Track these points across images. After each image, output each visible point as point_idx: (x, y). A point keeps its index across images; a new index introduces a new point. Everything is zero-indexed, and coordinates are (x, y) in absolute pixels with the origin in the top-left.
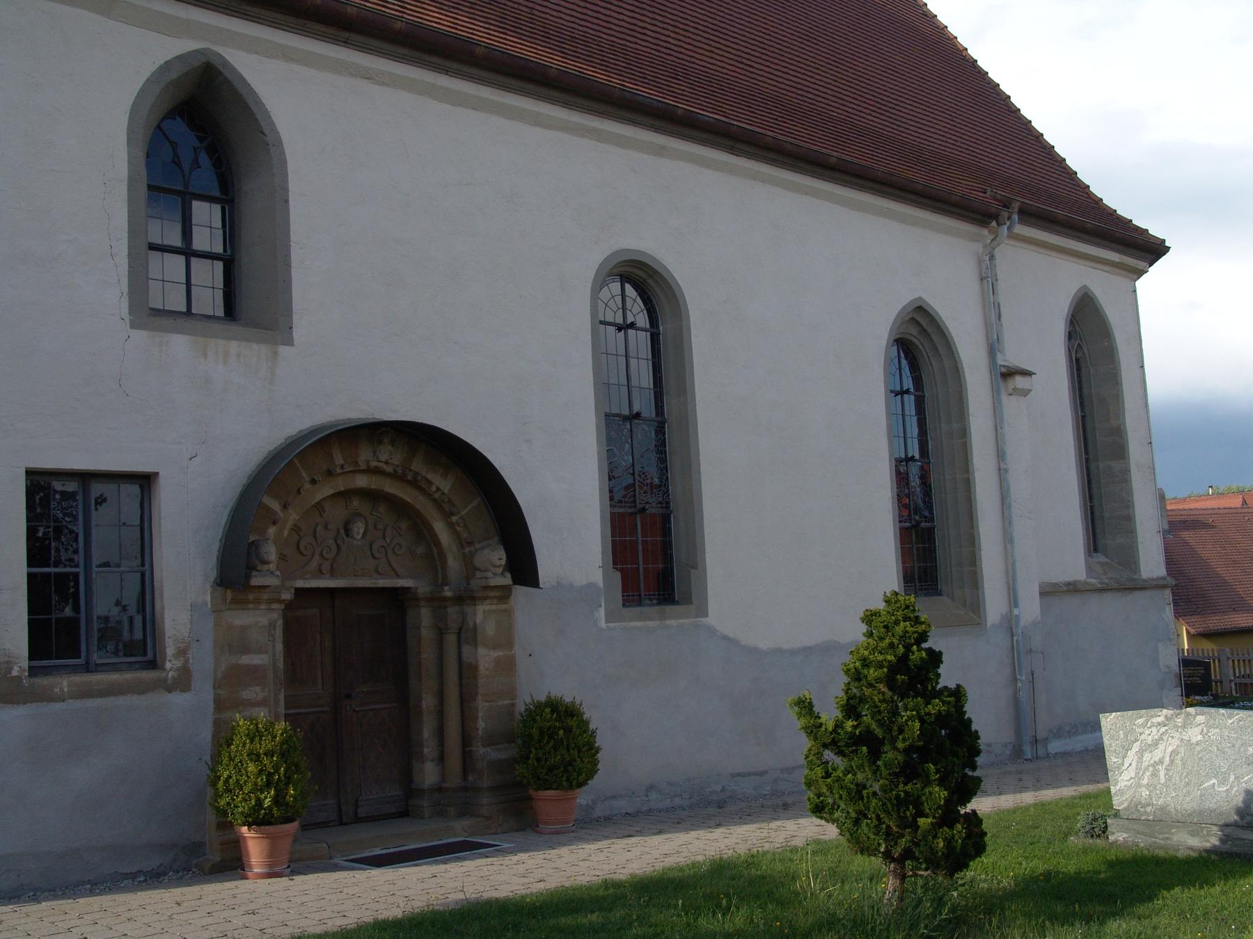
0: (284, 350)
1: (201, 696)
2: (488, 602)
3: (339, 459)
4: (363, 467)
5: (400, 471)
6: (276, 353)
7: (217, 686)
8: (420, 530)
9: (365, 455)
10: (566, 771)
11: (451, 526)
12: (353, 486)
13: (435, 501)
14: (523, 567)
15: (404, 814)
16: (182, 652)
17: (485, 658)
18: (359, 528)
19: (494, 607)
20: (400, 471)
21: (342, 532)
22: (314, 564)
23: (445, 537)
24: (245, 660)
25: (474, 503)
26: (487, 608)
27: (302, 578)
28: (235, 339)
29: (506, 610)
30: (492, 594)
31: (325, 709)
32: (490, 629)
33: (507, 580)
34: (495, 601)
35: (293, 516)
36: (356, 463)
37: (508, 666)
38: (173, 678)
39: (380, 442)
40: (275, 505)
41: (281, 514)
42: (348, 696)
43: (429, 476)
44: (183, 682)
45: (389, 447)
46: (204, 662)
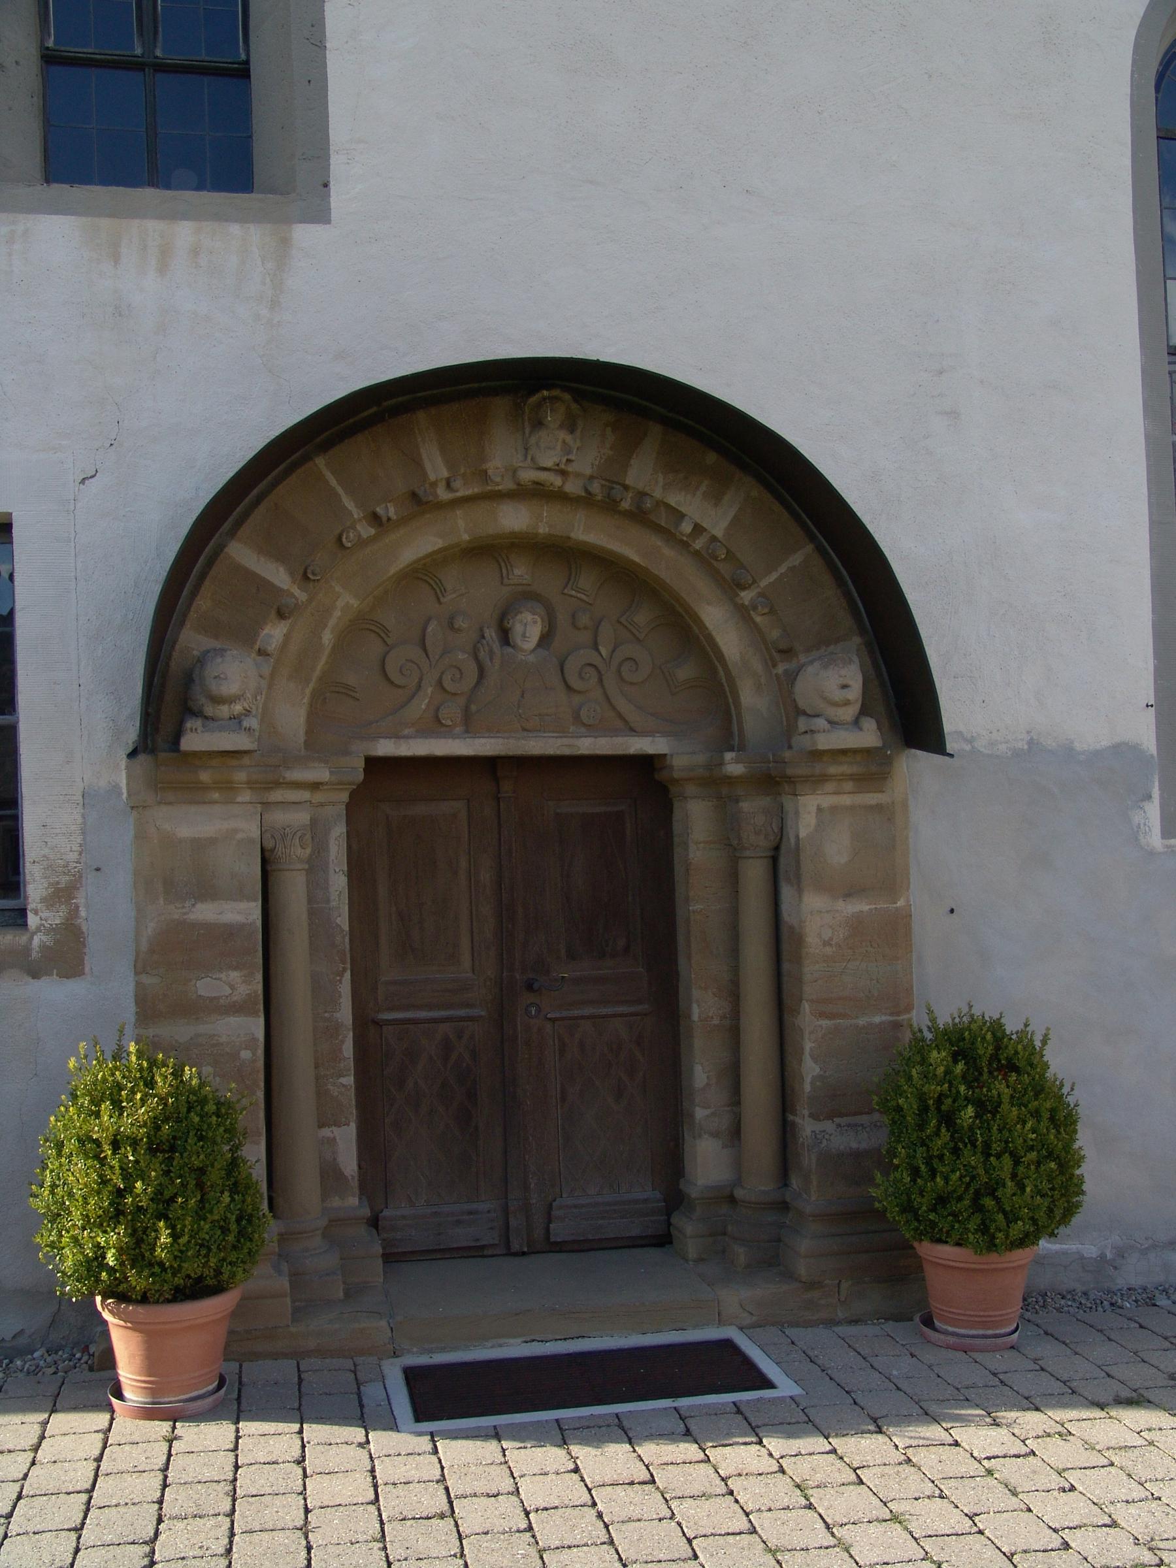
0: (305, 234)
1: (107, 988)
2: (830, 786)
3: (436, 467)
4: (508, 485)
5: (596, 488)
6: (285, 242)
7: (141, 967)
9: (504, 455)
10: (977, 1207)
11: (743, 613)
14: (909, 707)
15: (663, 1240)
16: (62, 894)
17: (818, 916)
18: (528, 628)
19: (846, 800)
20: (596, 488)
21: (491, 634)
22: (421, 705)
23: (731, 641)
24: (205, 912)
25: (796, 559)
26: (827, 801)
27: (397, 736)
28: (185, 217)
29: (879, 808)
30: (833, 770)
31: (475, 1012)
32: (837, 850)
33: (869, 736)
34: (849, 786)
35: (345, 601)
36: (484, 476)
37: (894, 933)
38: (44, 947)
39: (538, 424)
40: (279, 576)
41: (302, 596)
42: (530, 987)
43: (674, 499)
44: (66, 956)
45: (563, 435)
46: (114, 915)
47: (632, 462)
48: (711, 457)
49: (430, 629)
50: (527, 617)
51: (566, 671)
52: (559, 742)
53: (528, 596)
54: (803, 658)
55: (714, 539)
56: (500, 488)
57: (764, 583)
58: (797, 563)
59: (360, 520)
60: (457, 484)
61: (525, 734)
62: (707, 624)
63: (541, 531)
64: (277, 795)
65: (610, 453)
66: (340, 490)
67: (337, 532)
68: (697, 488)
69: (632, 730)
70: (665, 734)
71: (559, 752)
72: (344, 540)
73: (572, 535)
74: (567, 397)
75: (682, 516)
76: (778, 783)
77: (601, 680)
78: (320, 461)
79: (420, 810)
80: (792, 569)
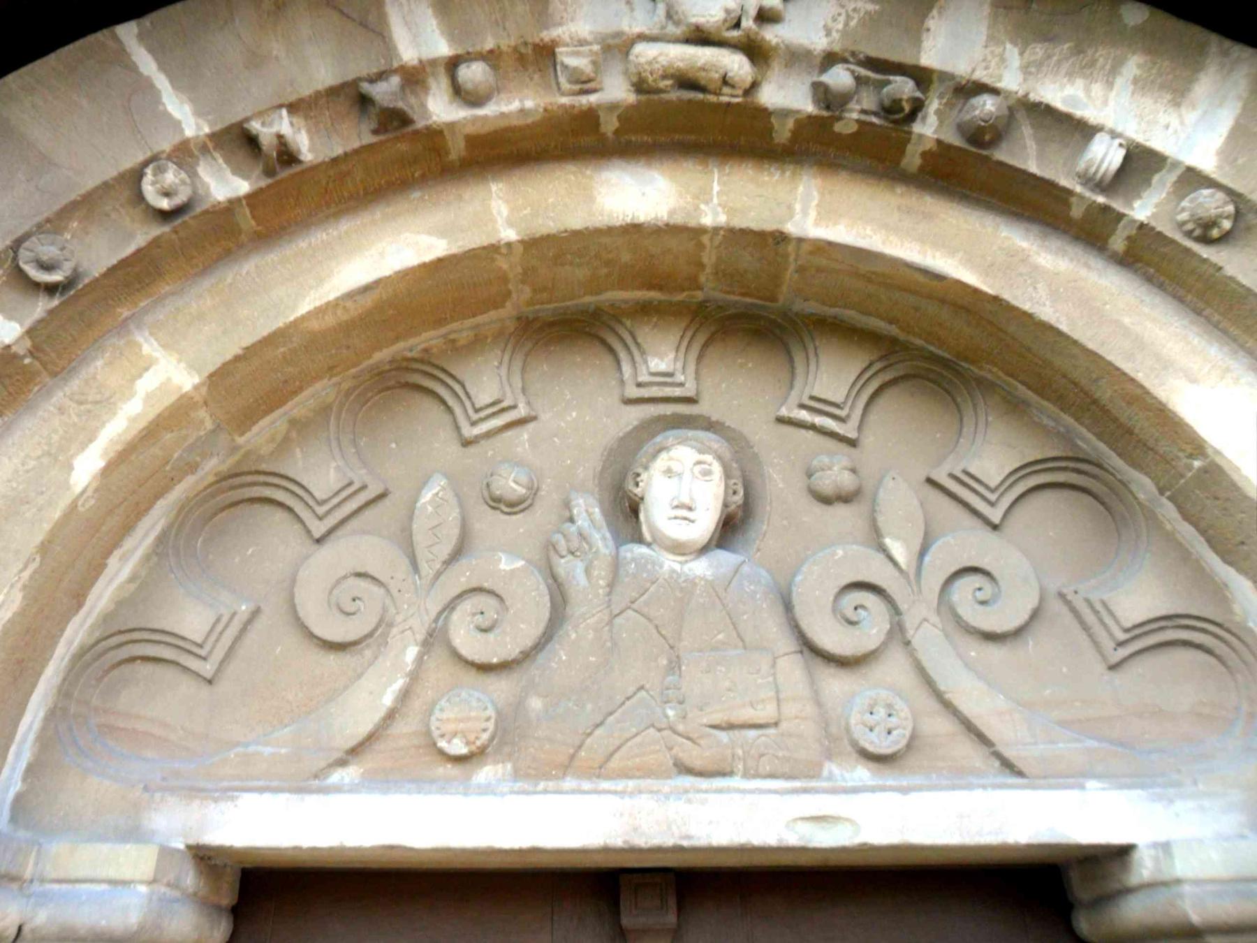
4: (615, 90)
12: (576, 220)
18: (684, 487)
21: (589, 512)
43: (1058, 93)
47: (931, 23)
49: (427, 496)
51: (798, 610)
53: (678, 416)
55: (1192, 179)
56: (593, 98)
59: (204, 149)
60: (474, 73)
61: (688, 781)
63: (707, 220)
67: (129, 162)
68: (1114, 71)
69: (1008, 766)
72: (149, 189)
73: (791, 228)
75: (1083, 131)
77: (898, 633)
78: (127, 32)
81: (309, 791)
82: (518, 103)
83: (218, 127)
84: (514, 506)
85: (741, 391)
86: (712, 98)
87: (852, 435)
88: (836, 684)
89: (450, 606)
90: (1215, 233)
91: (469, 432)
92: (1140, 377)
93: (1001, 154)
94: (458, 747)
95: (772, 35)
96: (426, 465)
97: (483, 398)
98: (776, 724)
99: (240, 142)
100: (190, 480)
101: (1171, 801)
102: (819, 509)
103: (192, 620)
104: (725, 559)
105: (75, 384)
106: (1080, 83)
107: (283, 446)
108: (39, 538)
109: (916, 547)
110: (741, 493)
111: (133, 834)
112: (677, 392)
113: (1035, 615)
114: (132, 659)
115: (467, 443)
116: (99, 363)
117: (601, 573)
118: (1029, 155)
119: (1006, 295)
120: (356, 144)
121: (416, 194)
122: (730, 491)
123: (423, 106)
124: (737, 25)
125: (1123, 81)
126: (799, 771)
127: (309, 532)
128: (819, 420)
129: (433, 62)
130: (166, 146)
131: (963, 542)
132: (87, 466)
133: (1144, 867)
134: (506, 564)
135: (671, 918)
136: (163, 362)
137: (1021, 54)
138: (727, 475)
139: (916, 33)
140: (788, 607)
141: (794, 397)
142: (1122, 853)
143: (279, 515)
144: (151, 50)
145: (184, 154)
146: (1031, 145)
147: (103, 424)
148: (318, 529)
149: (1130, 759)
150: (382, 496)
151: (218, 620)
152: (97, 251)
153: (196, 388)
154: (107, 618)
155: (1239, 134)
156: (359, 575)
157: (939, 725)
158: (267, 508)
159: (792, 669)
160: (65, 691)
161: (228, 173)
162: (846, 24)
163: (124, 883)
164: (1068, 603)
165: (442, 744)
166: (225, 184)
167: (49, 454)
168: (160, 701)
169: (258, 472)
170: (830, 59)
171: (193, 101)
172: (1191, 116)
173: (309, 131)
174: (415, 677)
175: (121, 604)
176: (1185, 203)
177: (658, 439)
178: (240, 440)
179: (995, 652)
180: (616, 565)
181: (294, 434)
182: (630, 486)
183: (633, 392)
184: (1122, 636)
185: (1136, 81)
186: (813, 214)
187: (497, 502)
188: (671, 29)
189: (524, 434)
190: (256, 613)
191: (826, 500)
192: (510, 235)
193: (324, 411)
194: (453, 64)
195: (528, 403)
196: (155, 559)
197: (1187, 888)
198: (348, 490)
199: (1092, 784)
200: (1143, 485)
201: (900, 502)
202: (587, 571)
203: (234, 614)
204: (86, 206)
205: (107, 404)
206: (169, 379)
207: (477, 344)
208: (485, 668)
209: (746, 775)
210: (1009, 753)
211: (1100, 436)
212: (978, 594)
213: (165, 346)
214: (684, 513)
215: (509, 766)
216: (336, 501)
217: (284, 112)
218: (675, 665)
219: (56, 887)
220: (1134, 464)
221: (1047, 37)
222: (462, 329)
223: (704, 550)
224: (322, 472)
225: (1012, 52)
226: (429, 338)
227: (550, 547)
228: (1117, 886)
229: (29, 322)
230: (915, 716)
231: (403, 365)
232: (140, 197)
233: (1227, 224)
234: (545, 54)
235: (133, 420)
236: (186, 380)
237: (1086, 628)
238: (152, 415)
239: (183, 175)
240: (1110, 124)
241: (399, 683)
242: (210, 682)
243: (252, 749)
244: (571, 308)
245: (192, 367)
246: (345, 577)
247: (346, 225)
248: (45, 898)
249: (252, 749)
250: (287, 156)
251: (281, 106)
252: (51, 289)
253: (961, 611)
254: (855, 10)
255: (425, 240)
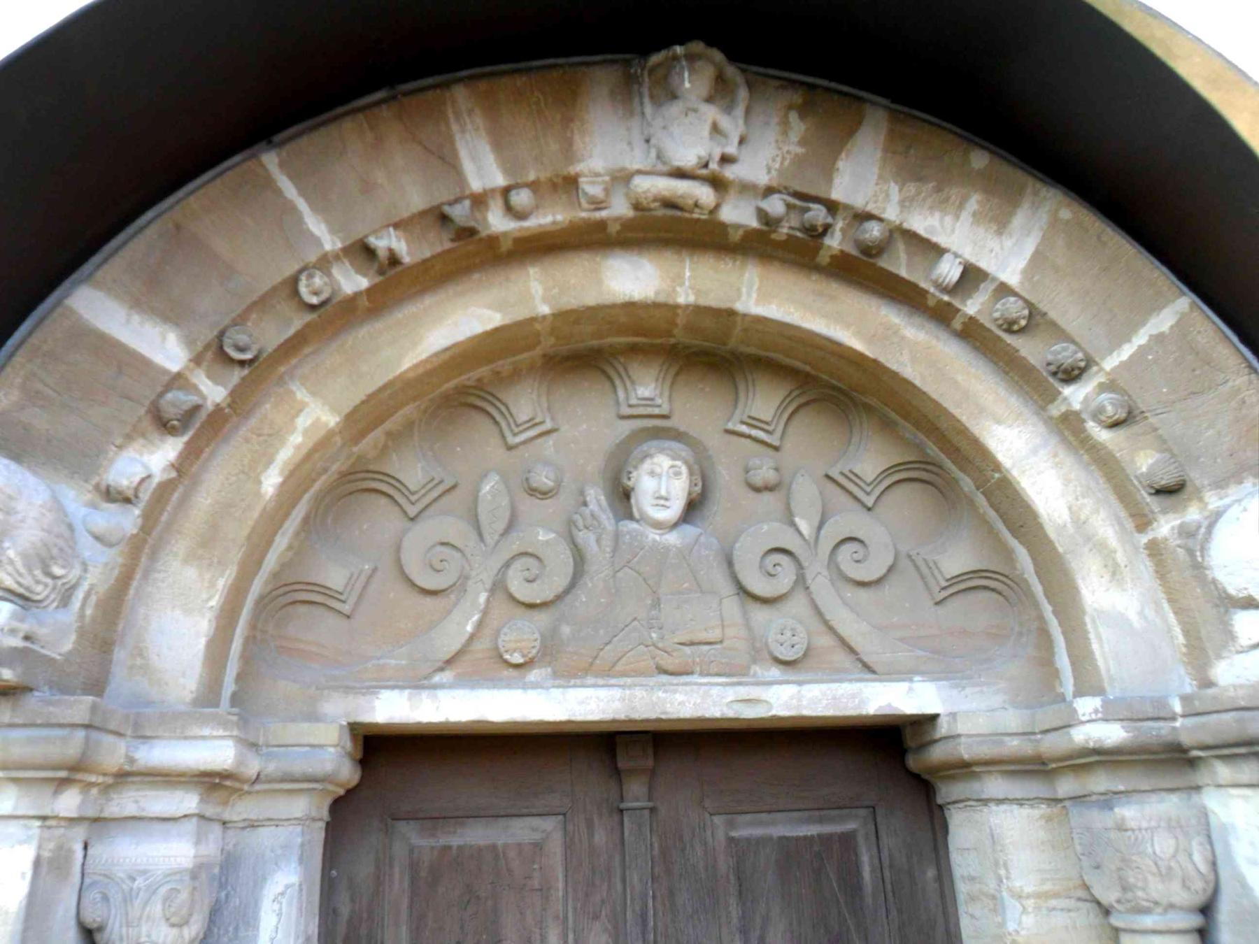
3: (482, 167)
4: (620, 208)
8: (941, 462)
11: (1069, 428)
12: (591, 299)
13: (972, 334)
18: (661, 482)
21: (597, 498)
25: (1164, 321)
40: (167, 349)
43: (921, 223)
45: (711, 113)
47: (841, 164)
48: (980, 159)
49: (486, 488)
50: (663, 462)
51: (737, 567)
52: (732, 694)
53: (659, 431)
54: (1213, 501)
55: (1003, 290)
56: (603, 214)
57: (1110, 363)
58: (1165, 328)
59: (337, 257)
60: (522, 198)
61: (665, 678)
62: (1000, 457)
63: (681, 300)
64: (127, 803)
65: (800, 150)
66: (302, 205)
68: (961, 207)
69: (868, 668)
70: (931, 675)
71: (730, 714)
72: (303, 290)
73: (739, 307)
74: (718, 56)
75: (937, 251)
76: (1192, 763)
77: (801, 581)
78: (270, 160)
79: (475, 835)
80: (1159, 339)
81: (423, 687)
82: (550, 217)
83: (348, 243)
84: (544, 494)
85: (700, 409)
86: (687, 215)
87: (776, 443)
88: (760, 615)
89: (507, 565)
90: (1016, 327)
91: (512, 440)
92: (964, 419)
93: (884, 263)
94: (517, 658)
95: (730, 172)
96: (482, 463)
97: (522, 417)
98: (721, 642)
99: (363, 252)
100: (324, 478)
101: (964, 688)
102: (752, 494)
103: (335, 577)
104: (689, 531)
105: (253, 422)
106: (937, 215)
107: (384, 451)
108: (246, 532)
109: (816, 524)
110: (700, 484)
111: (313, 717)
112: (656, 411)
113: (891, 570)
114: (295, 602)
115: (510, 448)
116: (268, 406)
117: (607, 543)
118: (900, 265)
119: (882, 360)
120: (439, 249)
121: (476, 276)
122: (693, 484)
123: (485, 219)
124: (706, 166)
125: (966, 216)
126: (734, 672)
127: (405, 513)
128: (754, 432)
129: (493, 191)
130: (312, 258)
131: (849, 521)
132: (271, 481)
133: (943, 728)
134: (542, 536)
135: (650, 762)
136: (312, 406)
137: (900, 191)
138: (691, 473)
139: (828, 172)
140: (730, 564)
141: (738, 415)
142: (933, 718)
143: (383, 501)
144: (291, 178)
145: (324, 263)
146: (903, 256)
147: (277, 451)
148: (412, 511)
149: (941, 663)
150: (454, 487)
151: (352, 575)
152: (269, 334)
153: (338, 424)
154: (275, 575)
155: (1038, 259)
156: (443, 544)
157: (825, 641)
158: (374, 496)
159: (732, 606)
160: (253, 626)
161: (352, 272)
162: (782, 163)
163: (321, 746)
164: (913, 561)
165: (507, 657)
166: (352, 282)
167: (243, 472)
168: (317, 630)
169: (368, 471)
170: (769, 191)
171: (327, 222)
172: (1008, 243)
173: (407, 242)
174: (485, 613)
175: (284, 566)
176: (998, 306)
177: (645, 447)
178: (355, 449)
179: (863, 594)
180: (617, 536)
181: (390, 443)
182: (625, 481)
183: (626, 411)
184: (944, 584)
185: (974, 215)
186: (754, 295)
187: (533, 492)
188: (660, 167)
189: (550, 441)
190: (375, 570)
191: (757, 490)
192: (545, 310)
193: (410, 425)
194: (506, 191)
195: (553, 419)
196: (303, 534)
197: (963, 740)
198: (432, 483)
199: (917, 678)
200: (967, 483)
201: (806, 491)
202: (598, 541)
203: (361, 571)
204: (262, 303)
205: (277, 436)
206: (318, 419)
207: (515, 375)
208: (531, 606)
209: (702, 674)
210: (865, 659)
211: (941, 449)
212: (855, 556)
213: (313, 394)
214: (662, 502)
215: (549, 670)
216: (423, 491)
217: (391, 229)
218: (657, 604)
219: (275, 749)
220: (962, 469)
221: (920, 179)
222: (505, 365)
223: (675, 525)
224: (413, 470)
225: (894, 189)
226: (483, 371)
227: (571, 523)
228: (929, 738)
229: (231, 386)
230: (809, 634)
231: (462, 391)
232: (296, 293)
233: (1023, 323)
234: (571, 183)
235: (298, 447)
236: (331, 420)
237: (923, 577)
238: (310, 445)
239: (326, 279)
240: (954, 248)
241: (476, 618)
242: (348, 617)
243: (382, 662)
244: (584, 352)
245: (334, 409)
246: (434, 546)
247: (429, 300)
248: (269, 756)
249: (382, 662)
250: (394, 260)
251: (388, 226)
252: (242, 363)
253: (842, 567)
254: (788, 152)
255: (487, 313)
